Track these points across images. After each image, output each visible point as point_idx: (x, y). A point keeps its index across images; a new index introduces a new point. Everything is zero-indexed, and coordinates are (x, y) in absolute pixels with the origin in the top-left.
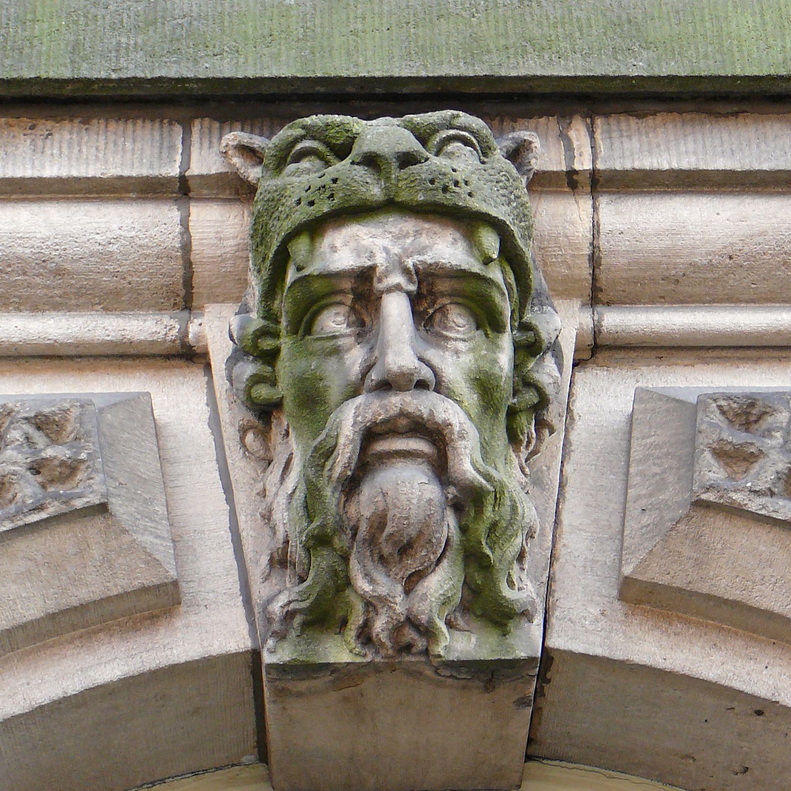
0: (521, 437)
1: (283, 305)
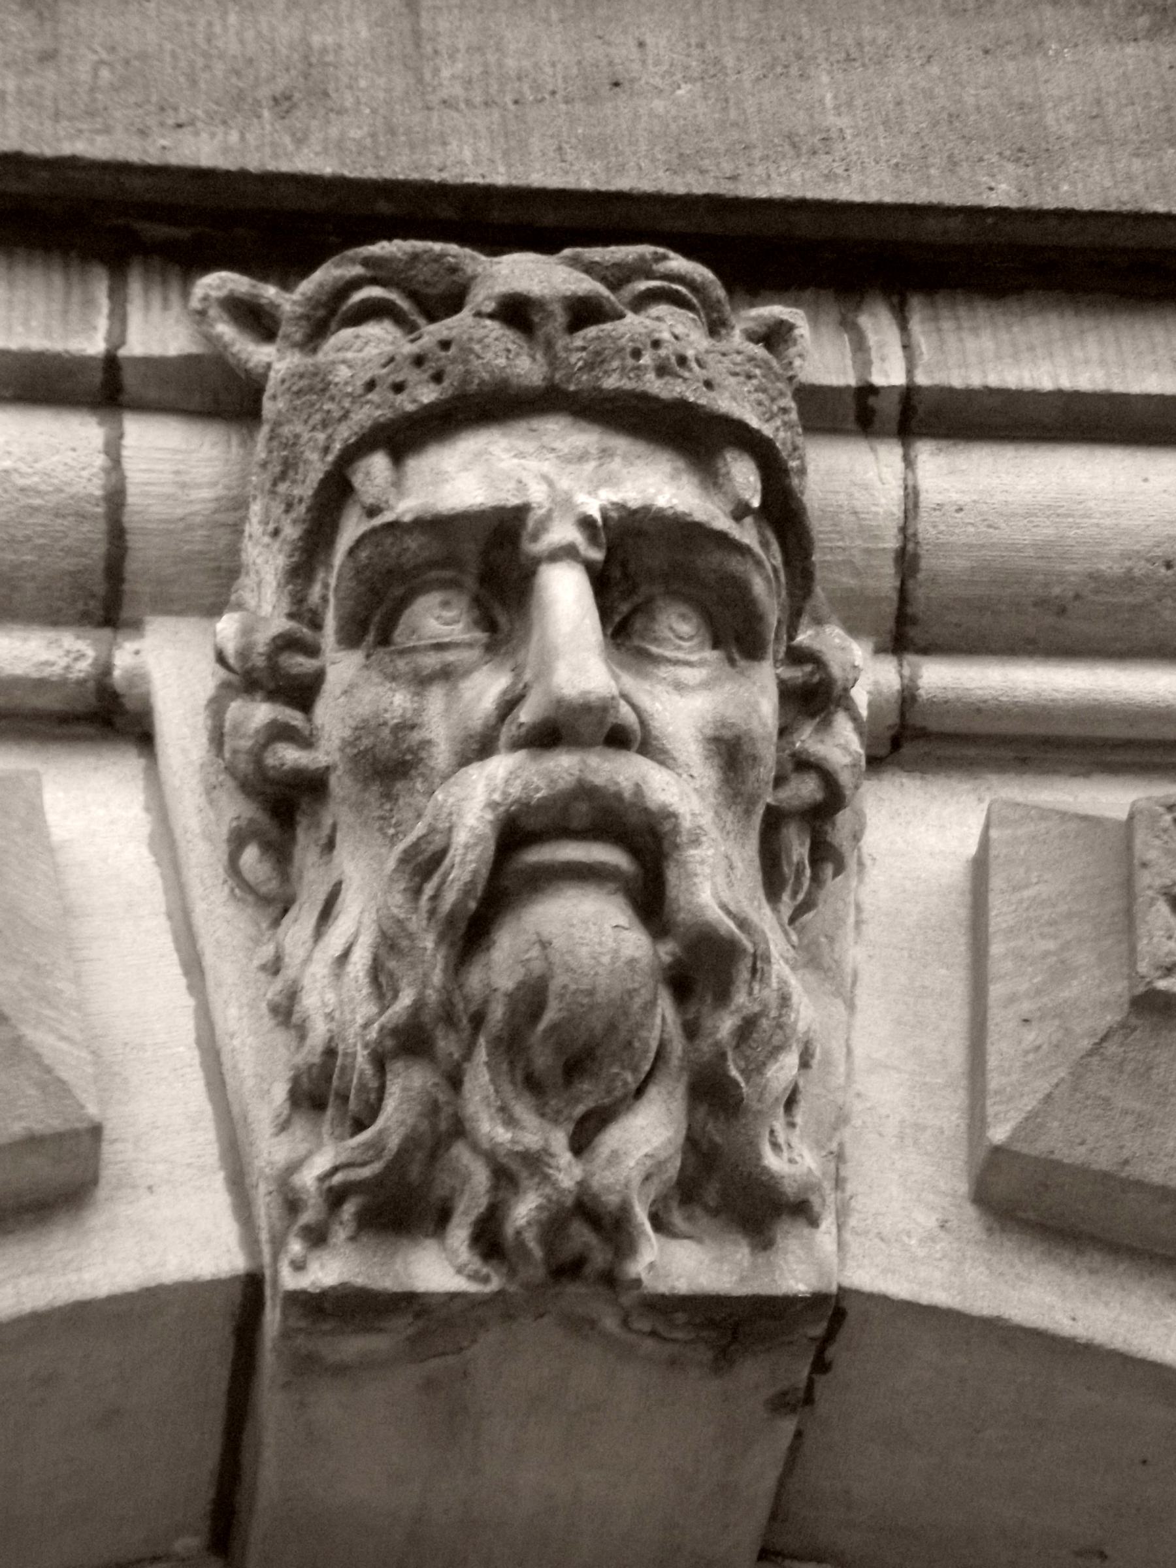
1: (331, 585)
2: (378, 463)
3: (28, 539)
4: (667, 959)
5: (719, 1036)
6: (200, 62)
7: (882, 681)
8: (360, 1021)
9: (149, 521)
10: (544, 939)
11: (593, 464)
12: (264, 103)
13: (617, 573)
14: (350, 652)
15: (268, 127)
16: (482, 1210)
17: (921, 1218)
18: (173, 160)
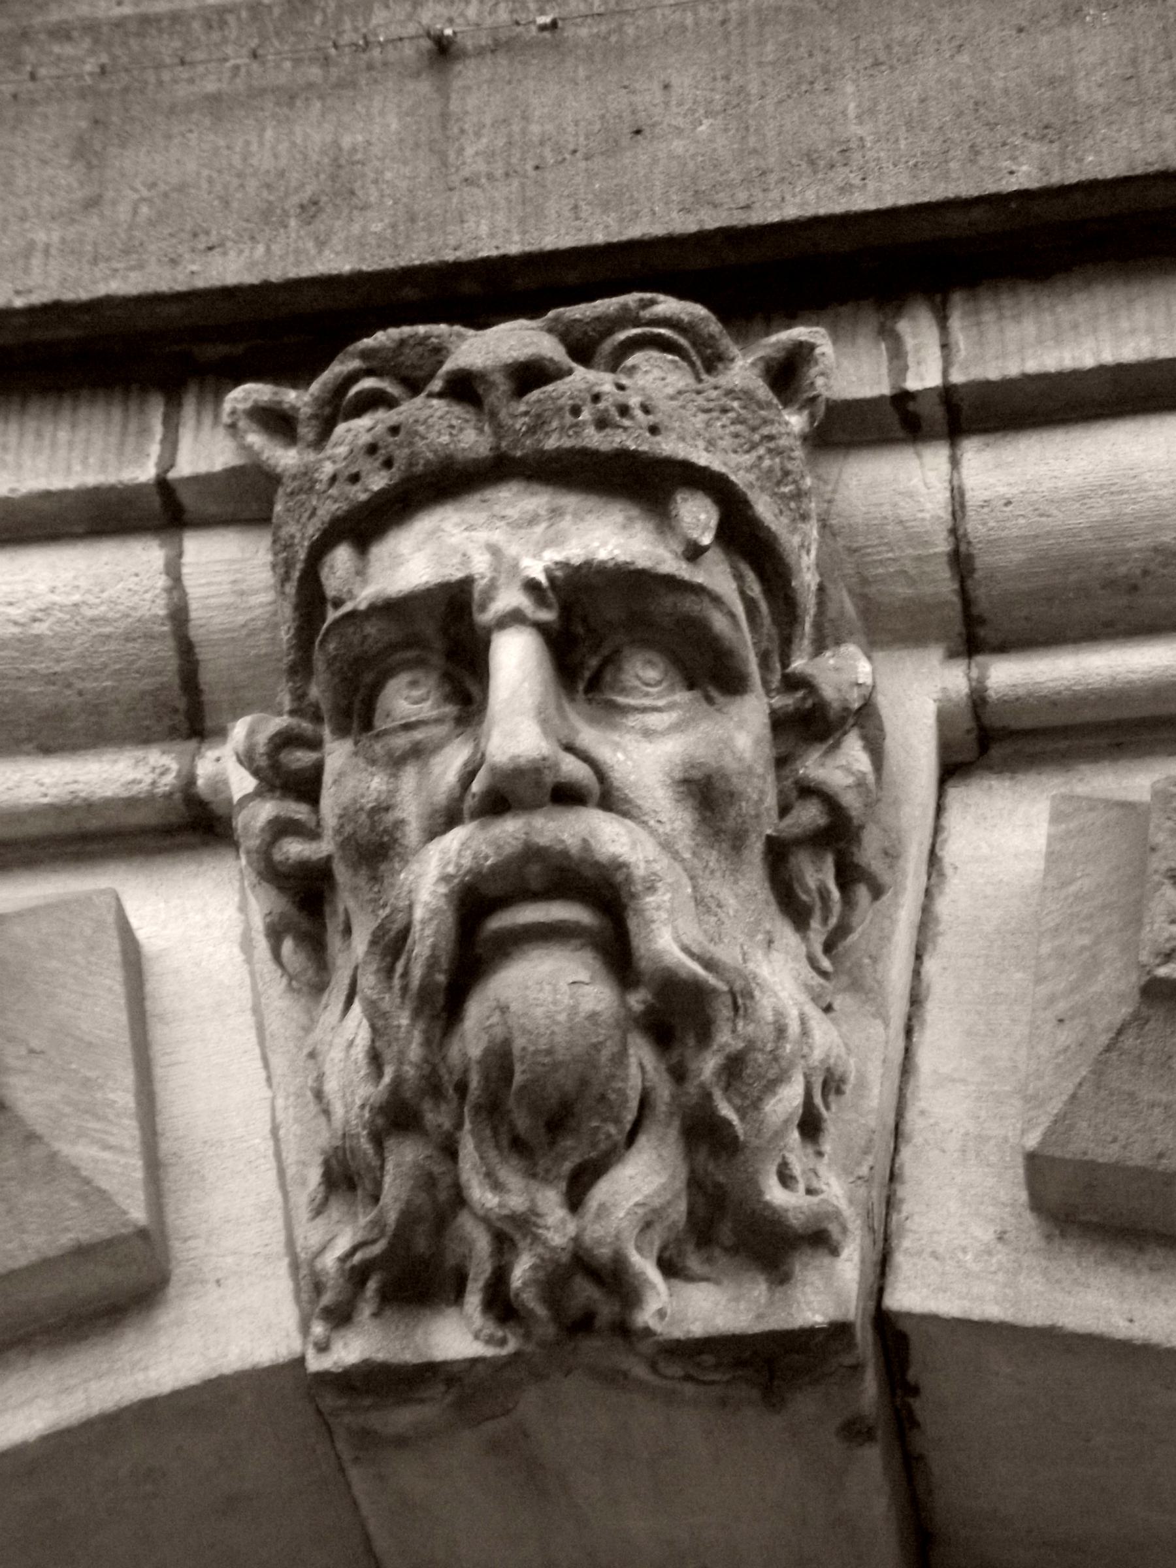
2: (342, 556)
3: (105, 666)
5: (702, 1078)
6: (236, 182)
7: (950, 686)
8: (358, 1102)
9: (214, 632)
11: (544, 525)
12: (292, 212)
13: (580, 630)
15: (293, 235)
16: (487, 1274)
18: (200, 284)
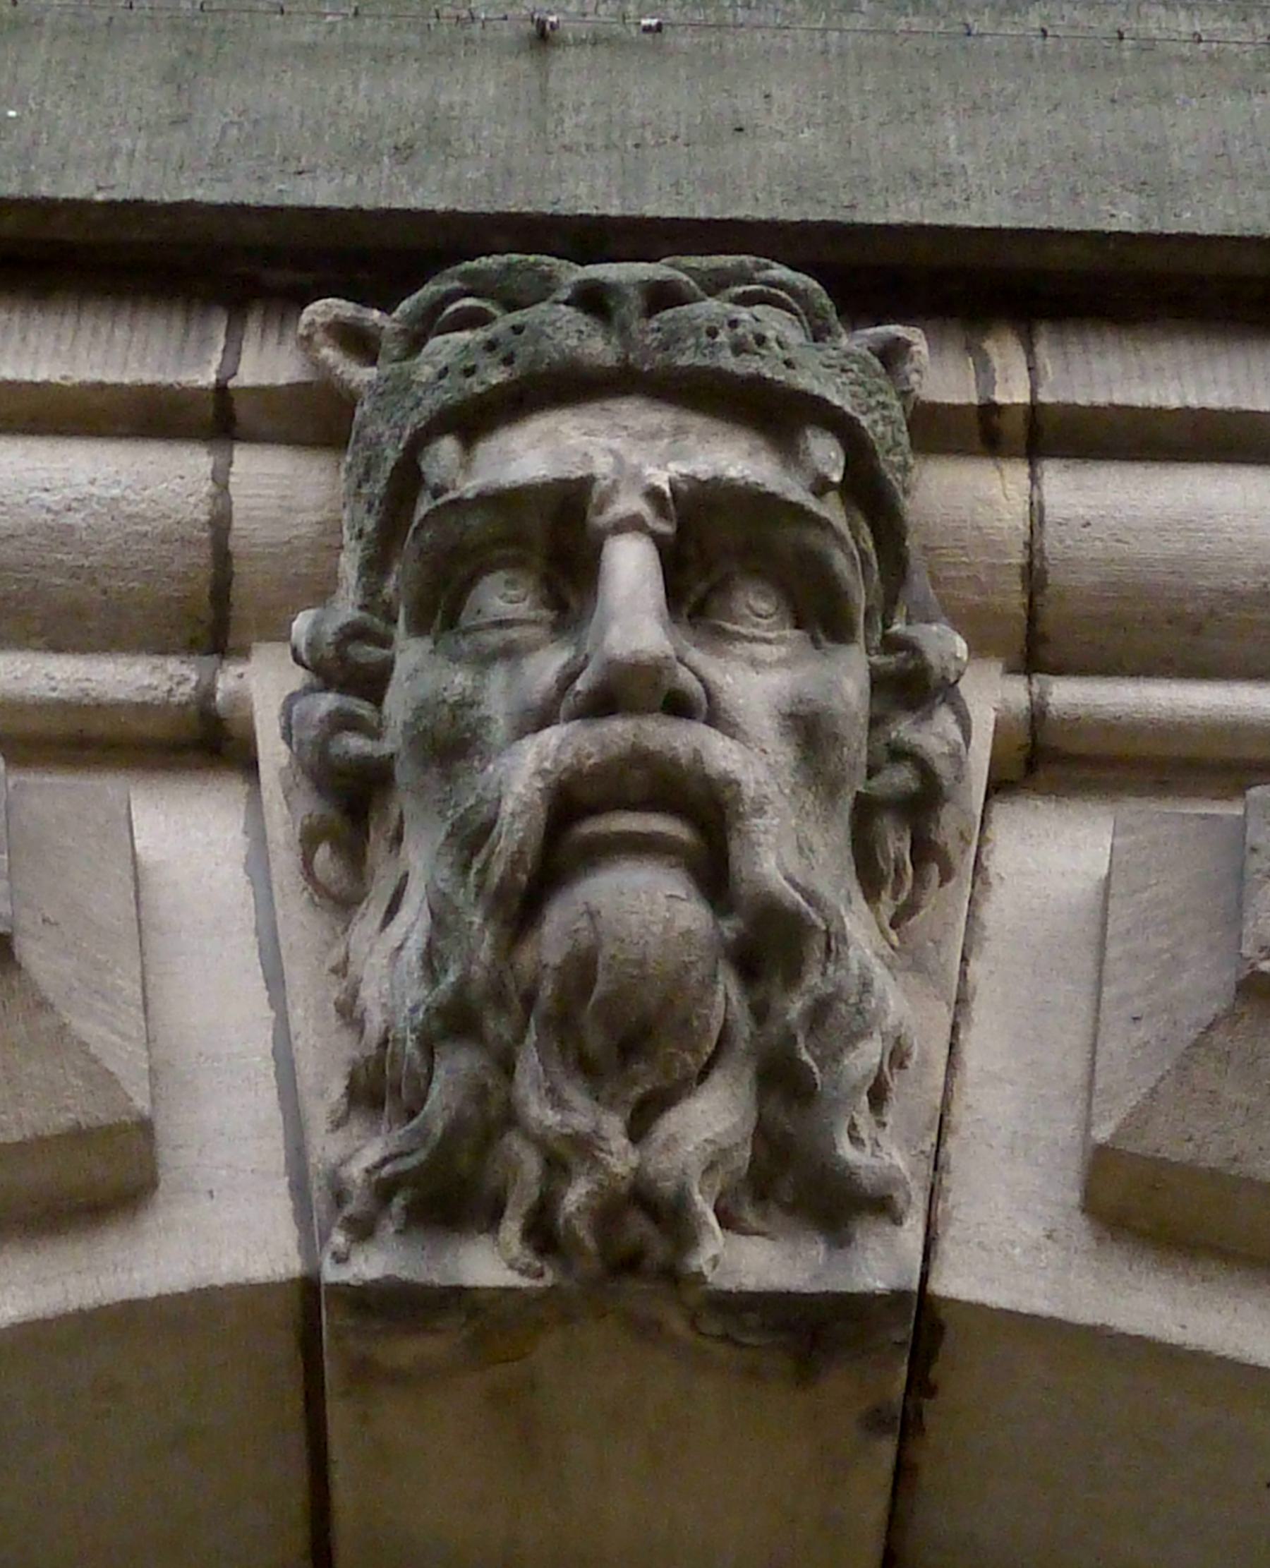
0: (882, 864)
2: (447, 448)
3: (135, 565)
4: (729, 935)
5: (788, 1018)
6: (328, 120)
8: (409, 1004)
9: (255, 545)
10: (593, 909)
13: (691, 551)
14: (419, 639)
15: (386, 171)
17: (1028, 1229)
18: (289, 201)
